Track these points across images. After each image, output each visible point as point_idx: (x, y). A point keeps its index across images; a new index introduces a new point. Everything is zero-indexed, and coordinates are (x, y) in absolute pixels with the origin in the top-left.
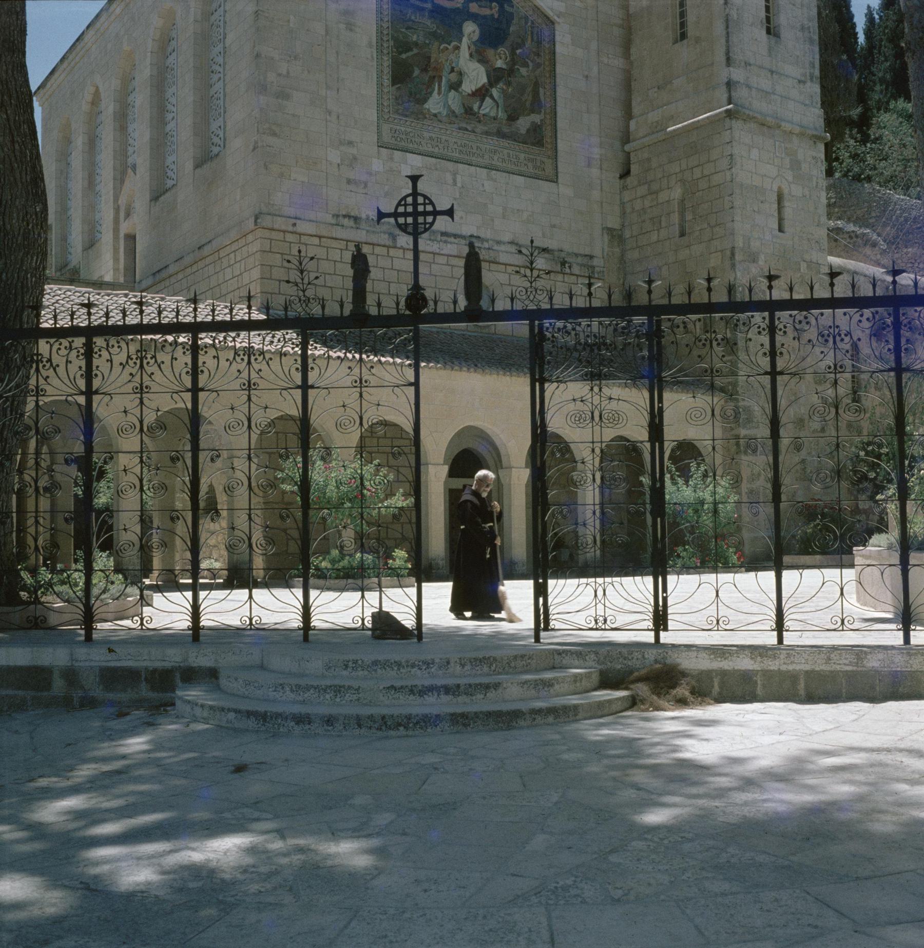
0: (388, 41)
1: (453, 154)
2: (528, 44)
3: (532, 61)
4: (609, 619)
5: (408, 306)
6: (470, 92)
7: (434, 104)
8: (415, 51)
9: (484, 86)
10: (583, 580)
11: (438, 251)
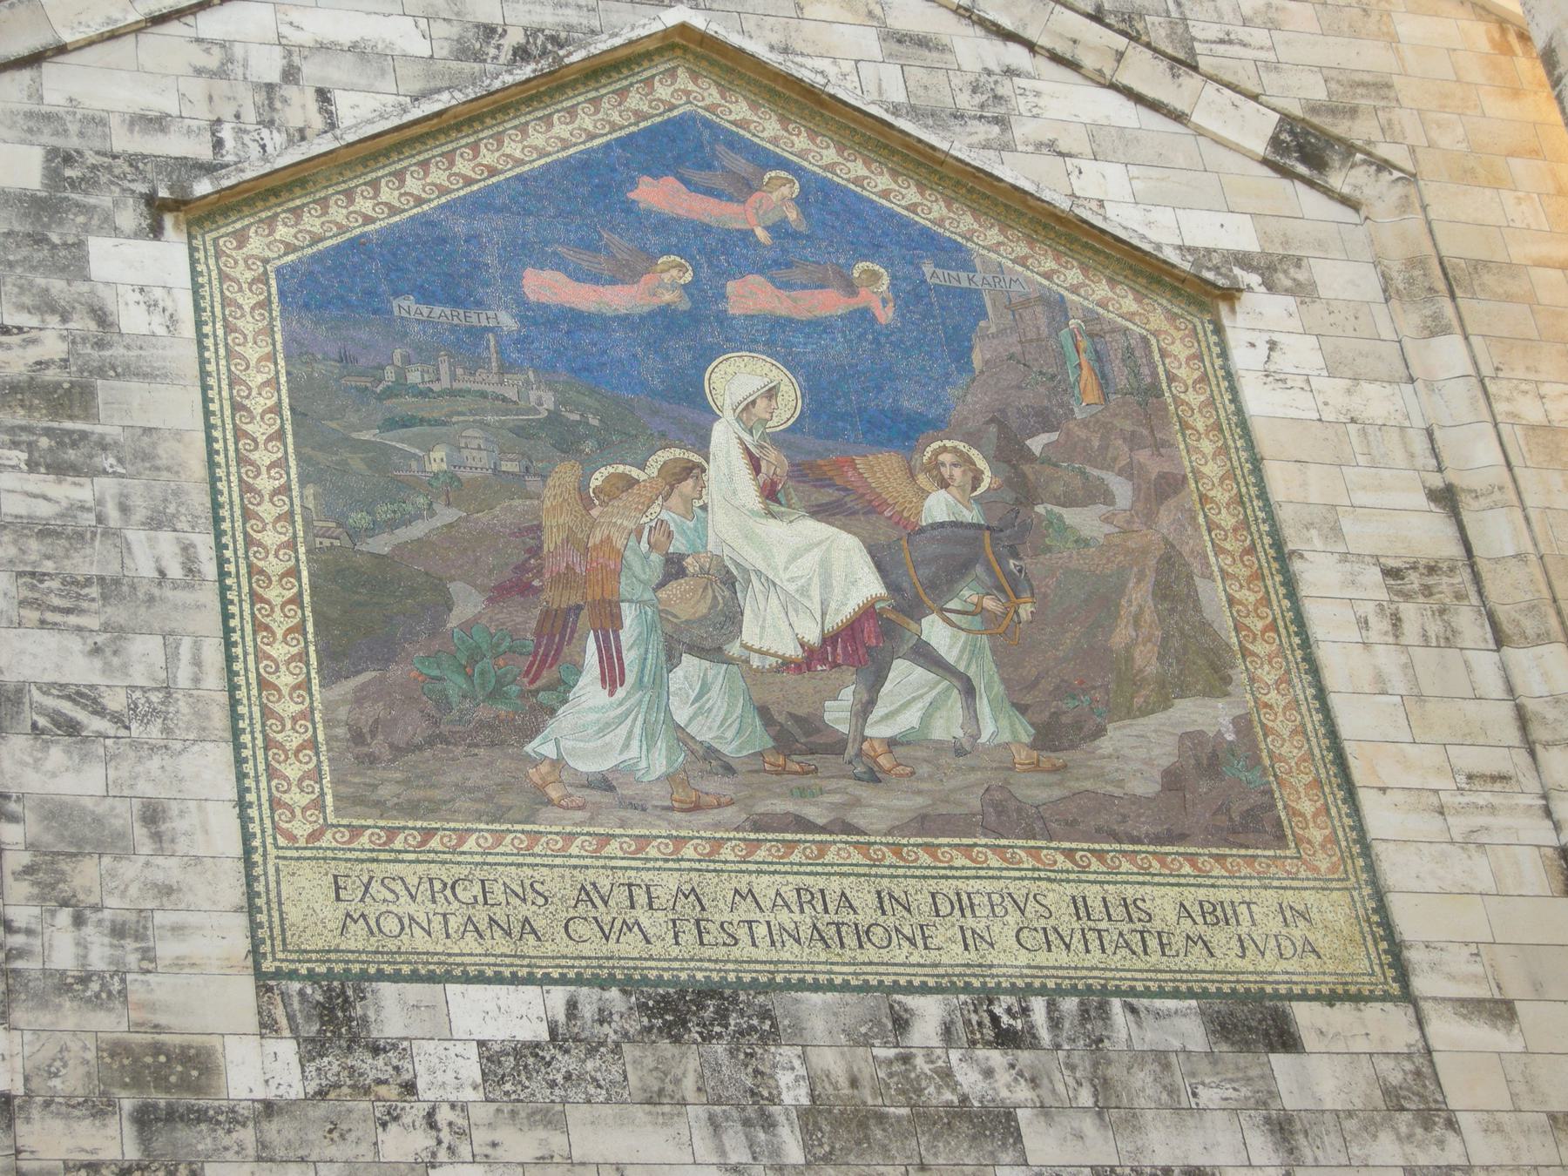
0: (286, 489)
1: (736, 952)
2: (1086, 401)
3: (1128, 472)
6: (792, 651)
8: (447, 515)
9: (868, 612)
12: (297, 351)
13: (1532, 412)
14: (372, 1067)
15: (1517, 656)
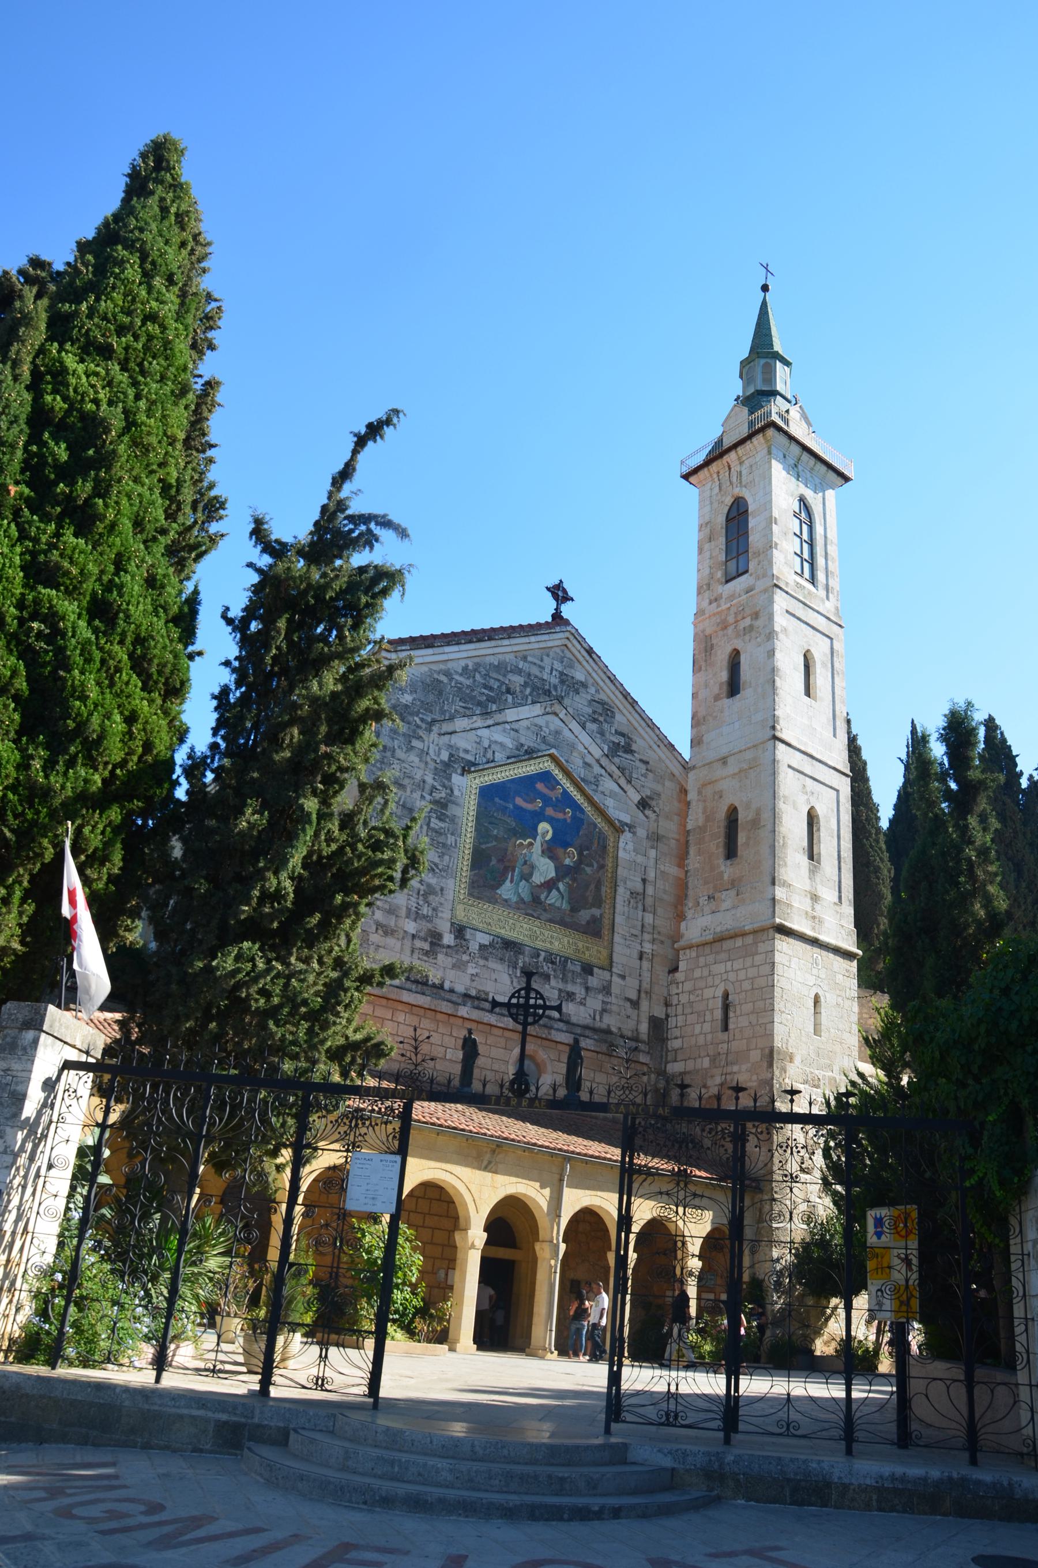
4: (681, 1414)
5: (511, 1089)
7: (506, 890)
8: (494, 843)
9: (552, 879)
10: (658, 1372)
11: (495, 1023)
12: (479, 805)
13: (662, 868)
14: (464, 943)
15: (646, 914)
